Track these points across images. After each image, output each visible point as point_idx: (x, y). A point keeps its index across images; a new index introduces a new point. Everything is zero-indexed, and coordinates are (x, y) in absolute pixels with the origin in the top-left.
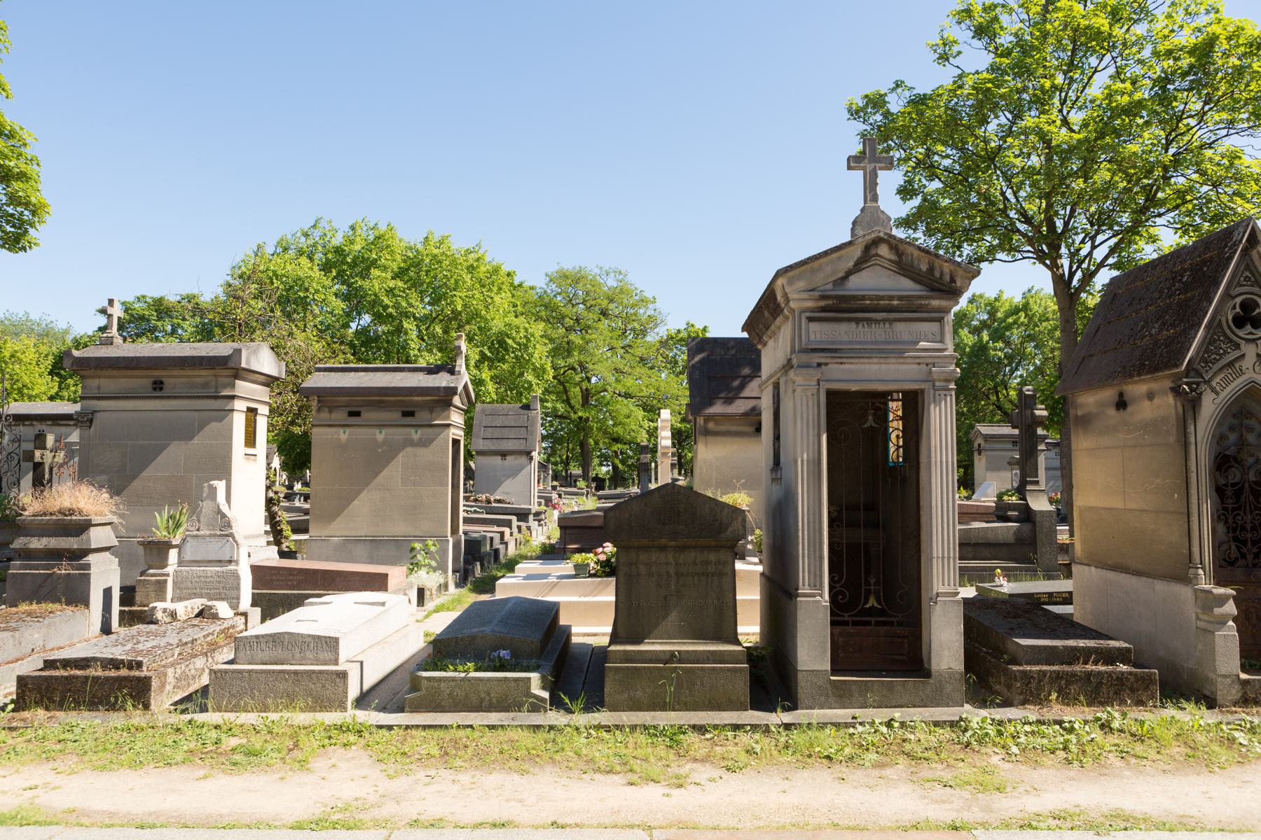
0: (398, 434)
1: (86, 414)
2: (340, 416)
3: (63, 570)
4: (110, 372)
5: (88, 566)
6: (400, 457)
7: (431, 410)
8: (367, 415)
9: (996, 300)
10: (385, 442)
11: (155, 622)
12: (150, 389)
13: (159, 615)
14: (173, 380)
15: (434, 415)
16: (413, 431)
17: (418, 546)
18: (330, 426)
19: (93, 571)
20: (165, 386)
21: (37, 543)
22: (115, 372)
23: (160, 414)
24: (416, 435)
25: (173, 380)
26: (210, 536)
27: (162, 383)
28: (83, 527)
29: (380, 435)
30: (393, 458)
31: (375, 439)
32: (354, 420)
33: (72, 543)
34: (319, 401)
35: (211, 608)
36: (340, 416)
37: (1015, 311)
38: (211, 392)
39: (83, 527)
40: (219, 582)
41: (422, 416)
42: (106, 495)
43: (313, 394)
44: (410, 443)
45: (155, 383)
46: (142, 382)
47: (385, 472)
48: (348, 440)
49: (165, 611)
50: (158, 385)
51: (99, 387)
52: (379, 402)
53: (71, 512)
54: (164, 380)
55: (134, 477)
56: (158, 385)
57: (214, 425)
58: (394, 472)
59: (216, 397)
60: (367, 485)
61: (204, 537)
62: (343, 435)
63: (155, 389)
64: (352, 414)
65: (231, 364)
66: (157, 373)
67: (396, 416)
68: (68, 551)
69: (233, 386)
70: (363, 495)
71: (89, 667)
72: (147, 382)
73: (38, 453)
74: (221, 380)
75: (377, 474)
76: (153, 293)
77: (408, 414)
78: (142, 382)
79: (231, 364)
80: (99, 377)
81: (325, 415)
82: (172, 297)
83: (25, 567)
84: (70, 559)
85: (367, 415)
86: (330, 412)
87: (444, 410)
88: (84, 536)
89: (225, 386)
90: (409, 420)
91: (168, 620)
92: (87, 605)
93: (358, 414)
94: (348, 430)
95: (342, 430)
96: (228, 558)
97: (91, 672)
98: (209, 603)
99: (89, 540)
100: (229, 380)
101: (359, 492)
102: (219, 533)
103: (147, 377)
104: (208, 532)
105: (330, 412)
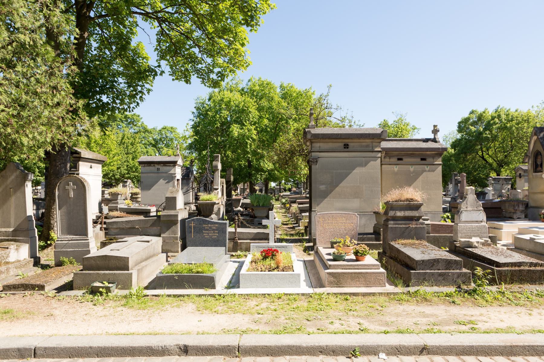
0: (419, 168)
2: (394, 160)
3: (413, 225)
4: (327, 140)
6: (421, 178)
8: (406, 160)
9: (484, 112)
10: (414, 172)
12: (343, 147)
15: (435, 160)
16: (426, 167)
18: (390, 164)
21: (399, 214)
23: (348, 159)
24: (427, 168)
25: (353, 144)
27: (348, 145)
28: (417, 207)
29: (412, 169)
31: (410, 170)
34: (386, 154)
36: (394, 160)
37: (493, 118)
38: (370, 149)
41: (429, 160)
44: (425, 171)
45: (345, 145)
46: (339, 145)
50: (346, 146)
51: (320, 147)
52: (412, 154)
54: (349, 144)
55: (337, 186)
56: (346, 146)
57: (372, 162)
61: (470, 211)
62: (396, 168)
63: (345, 148)
64: (399, 159)
66: (347, 141)
68: (415, 217)
74: (374, 144)
78: (339, 145)
80: (320, 142)
81: (387, 160)
86: (390, 158)
88: (419, 211)
90: (423, 162)
94: (398, 166)
95: (395, 166)
97: (522, 268)
100: (378, 144)
103: (342, 142)
105: (390, 158)
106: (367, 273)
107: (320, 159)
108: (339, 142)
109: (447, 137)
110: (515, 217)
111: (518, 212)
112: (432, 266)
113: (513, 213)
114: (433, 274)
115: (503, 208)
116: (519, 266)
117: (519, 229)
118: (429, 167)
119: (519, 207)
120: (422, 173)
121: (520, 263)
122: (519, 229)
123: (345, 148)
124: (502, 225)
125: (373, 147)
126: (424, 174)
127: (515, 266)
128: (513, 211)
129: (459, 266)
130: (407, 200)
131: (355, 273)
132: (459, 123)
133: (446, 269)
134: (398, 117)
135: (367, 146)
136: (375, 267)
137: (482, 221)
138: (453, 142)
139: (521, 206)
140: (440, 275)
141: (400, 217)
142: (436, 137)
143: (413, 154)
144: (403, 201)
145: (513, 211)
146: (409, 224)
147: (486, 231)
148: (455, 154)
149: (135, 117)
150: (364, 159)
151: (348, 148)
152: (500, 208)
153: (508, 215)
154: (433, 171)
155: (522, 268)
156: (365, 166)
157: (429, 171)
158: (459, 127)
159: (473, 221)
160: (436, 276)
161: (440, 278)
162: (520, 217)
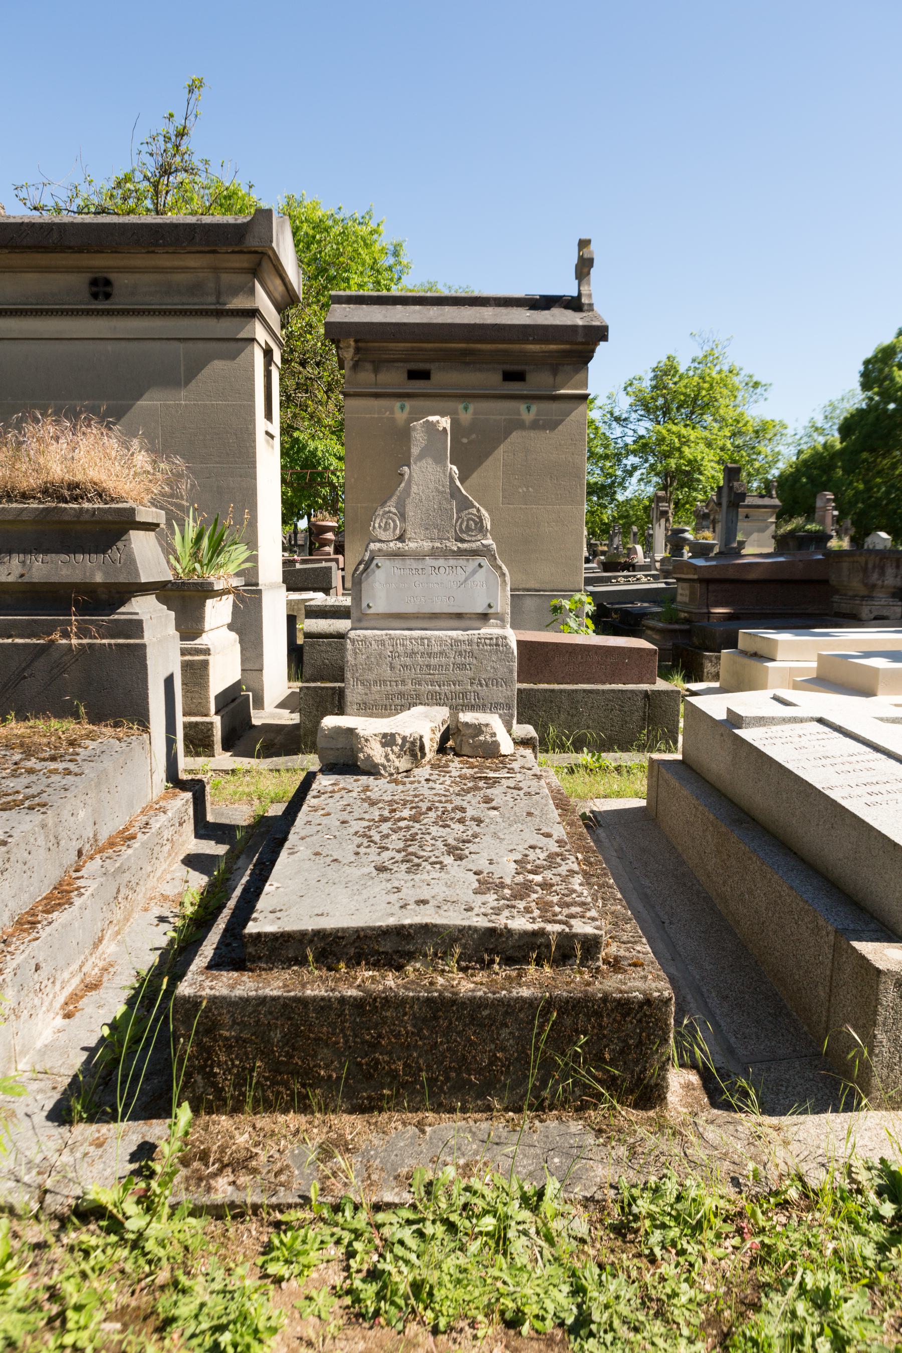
2: (394, 378)
5: (135, 627)
7: (555, 370)
8: (442, 377)
11: (372, 770)
13: (376, 752)
14: (132, 277)
15: (560, 378)
16: (523, 407)
17: (567, 604)
18: (377, 396)
19: (149, 637)
20: (116, 291)
22: (16, 259)
23: (110, 347)
24: (528, 413)
25: (132, 277)
26: (434, 553)
27: (108, 283)
28: (110, 528)
32: (418, 386)
34: (357, 350)
35: (478, 729)
36: (394, 378)
38: (209, 301)
39: (110, 528)
40: (462, 667)
41: (538, 380)
42: (142, 459)
43: (348, 335)
44: (520, 425)
45: (94, 282)
46: (66, 280)
49: (388, 740)
50: (101, 288)
52: (465, 353)
54: (113, 277)
56: (101, 288)
57: (217, 365)
61: (418, 556)
63: (95, 296)
64: (414, 375)
65: (252, 242)
67: (492, 379)
69: (252, 292)
71: (411, 956)
72: (80, 281)
74: (225, 278)
79: (252, 242)
81: (366, 376)
85: (442, 377)
86: (376, 371)
87: (577, 371)
89: (235, 291)
90: (515, 387)
91: (403, 763)
92: (144, 722)
93: (424, 375)
94: (408, 404)
95: (397, 404)
96: (480, 609)
98: (466, 717)
99: (131, 563)
102: (454, 546)
103: (79, 270)
104: (427, 545)
105: (376, 371)
108: (68, 270)
109: (834, 409)
110: (865, 612)
111: (878, 594)
113: (863, 598)
115: (834, 580)
117: (820, 657)
118: (534, 408)
119: (882, 573)
120: (507, 434)
121: (400, 932)
122: (820, 657)
123: (95, 296)
124: (775, 642)
125: (219, 294)
126: (515, 436)
127: (355, 961)
128: (863, 591)
130: (49, 491)
132: (867, 363)
134: (707, 348)
135: (195, 289)
137: (484, 617)
138: (846, 419)
139: (890, 571)
142: (585, 290)
143: (471, 352)
144: (24, 496)
145: (863, 591)
147: (502, 671)
148: (842, 451)
150: (181, 346)
151: (108, 296)
152: (826, 582)
153: (845, 608)
154: (553, 425)
156: (188, 382)
157: (536, 425)
158: (865, 375)
159: (434, 616)
162: (885, 612)
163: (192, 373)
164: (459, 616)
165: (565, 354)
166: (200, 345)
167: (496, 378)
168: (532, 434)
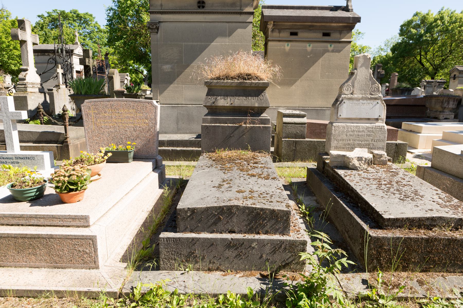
0: (320, 46)
1: (155, 24)
2: (285, 35)
3: (247, 124)
6: (320, 61)
7: (340, 33)
9: (428, 14)
10: (312, 51)
12: (196, 7)
15: (342, 35)
16: (329, 45)
18: (279, 41)
20: (206, 5)
23: (203, 24)
26: (362, 99)
28: (258, 90)
29: (309, 47)
30: (316, 61)
31: (306, 50)
32: (293, 38)
33: (253, 102)
34: (274, 25)
36: (285, 35)
37: (436, 20)
38: (237, 9)
40: (369, 136)
41: (335, 36)
43: (272, 20)
45: (199, 2)
47: (311, 70)
48: (290, 50)
52: (311, 26)
53: (249, 76)
55: (188, 66)
57: (239, 31)
58: (316, 70)
59: (241, 13)
60: (301, 77)
61: (358, 99)
62: (287, 47)
63: (199, 7)
64: (292, 34)
67: (319, 35)
68: (253, 108)
70: (298, 83)
71: (435, 226)
73: (87, 60)
75: (306, 71)
76: (60, 8)
77: (326, 35)
82: (67, 11)
83: (216, 121)
84: (253, 115)
85: (302, 35)
86: (279, 32)
87: (348, 33)
88: (260, 97)
90: (326, 38)
94: (290, 44)
97: (434, 233)
101: (295, 81)
102: (369, 96)
104: (360, 96)
105: (279, 32)
106: (51, 237)
107: (162, 24)
109: (389, 42)
110: (441, 117)
111: (446, 111)
112: (215, 223)
113: (440, 112)
114: (211, 243)
115: (427, 105)
116: (429, 228)
117: (444, 133)
118: (333, 46)
119: (448, 103)
120: (323, 54)
121: (433, 219)
122: (444, 133)
123: (199, 7)
124: (421, 127)
125: (241, 7)
126: (326, 55)
127: (419, 227)
128: (440, 109)
129: (281, 225)
130: (240, 76)
131: (24, 237)
132: (402, 26)
133: (250, 231)
136: (78, 223)
137: (377, 119)
138: (394, 46)
139: (451, 103)
140: (230, 244)
141: (224, 108)
142: (349, 4)
144: (232, 78)
145: (440, 109)
146: (240, 121)
147: (382, 137)
148: (393, 58)
149: (87, 17)
150: (227, 24)
151: (203, 7)
152: (424, 106)
153: (432, 115)
154: (339, 51)
155: (434, 233)
157: (333, 51)
158: (401, 30)
159: (361, 119)
160: (220, 248)
161: (230, 253)
162: (448, 117)
163: (230, 33)
164: (369, 119)
165: (345, 27)
166: (234, 24)
167: (320, 35)
168: (332, 54)
